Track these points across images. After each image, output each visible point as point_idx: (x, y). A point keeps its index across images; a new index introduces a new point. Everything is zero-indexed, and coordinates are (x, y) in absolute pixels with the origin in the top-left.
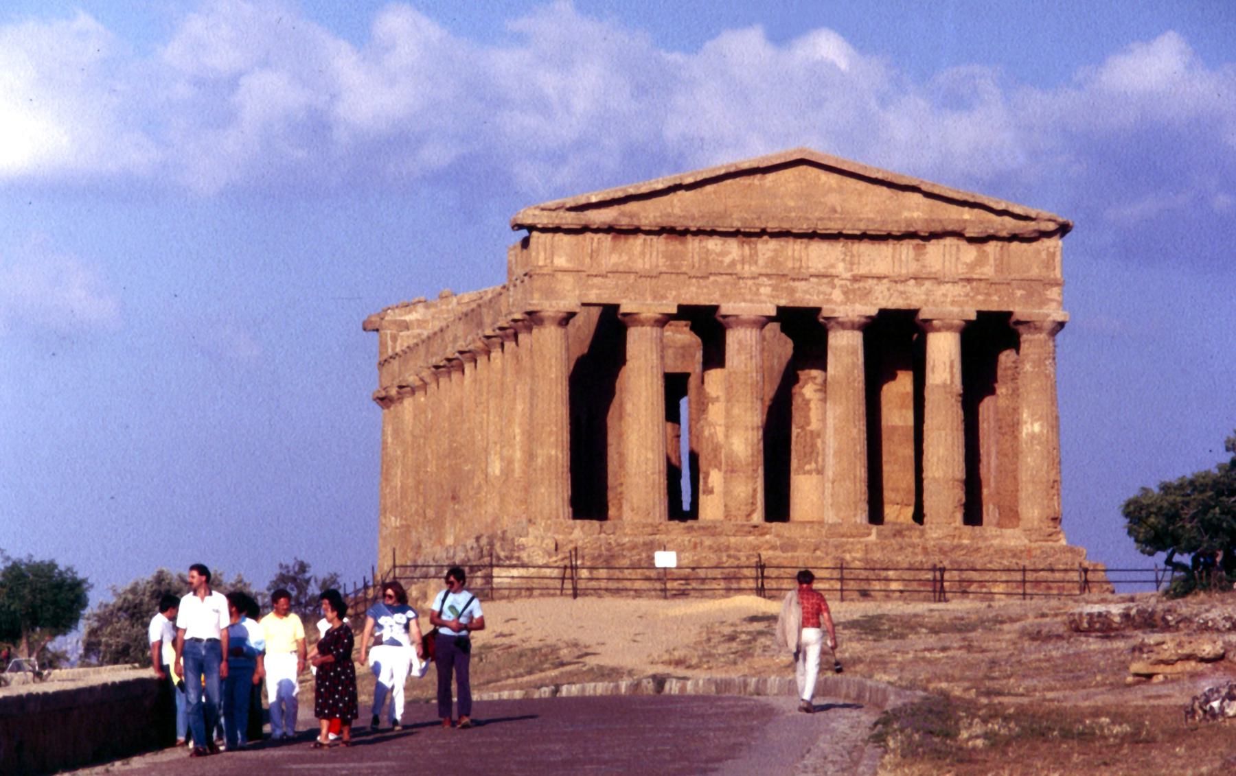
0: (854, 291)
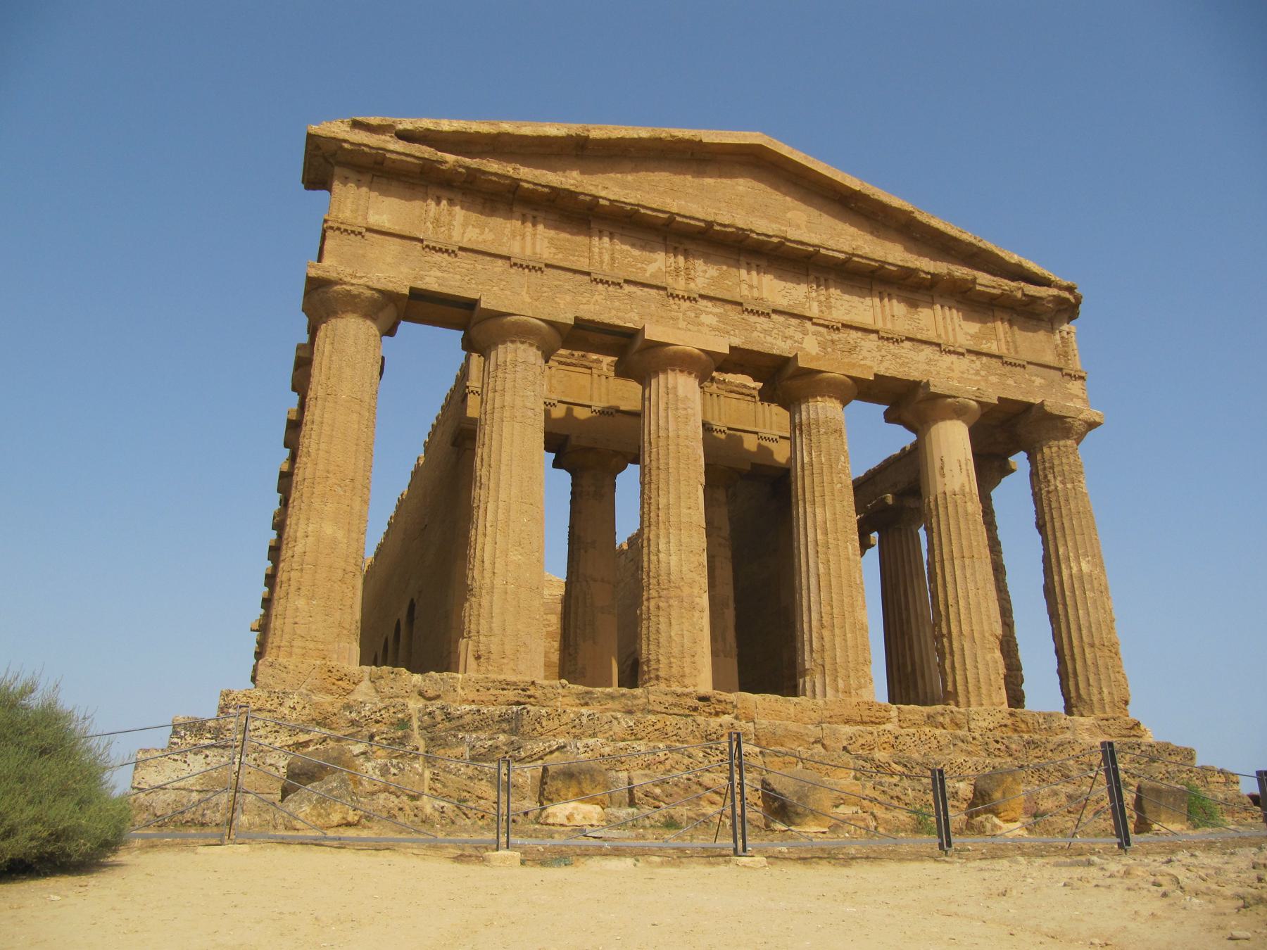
0: (833, 342)
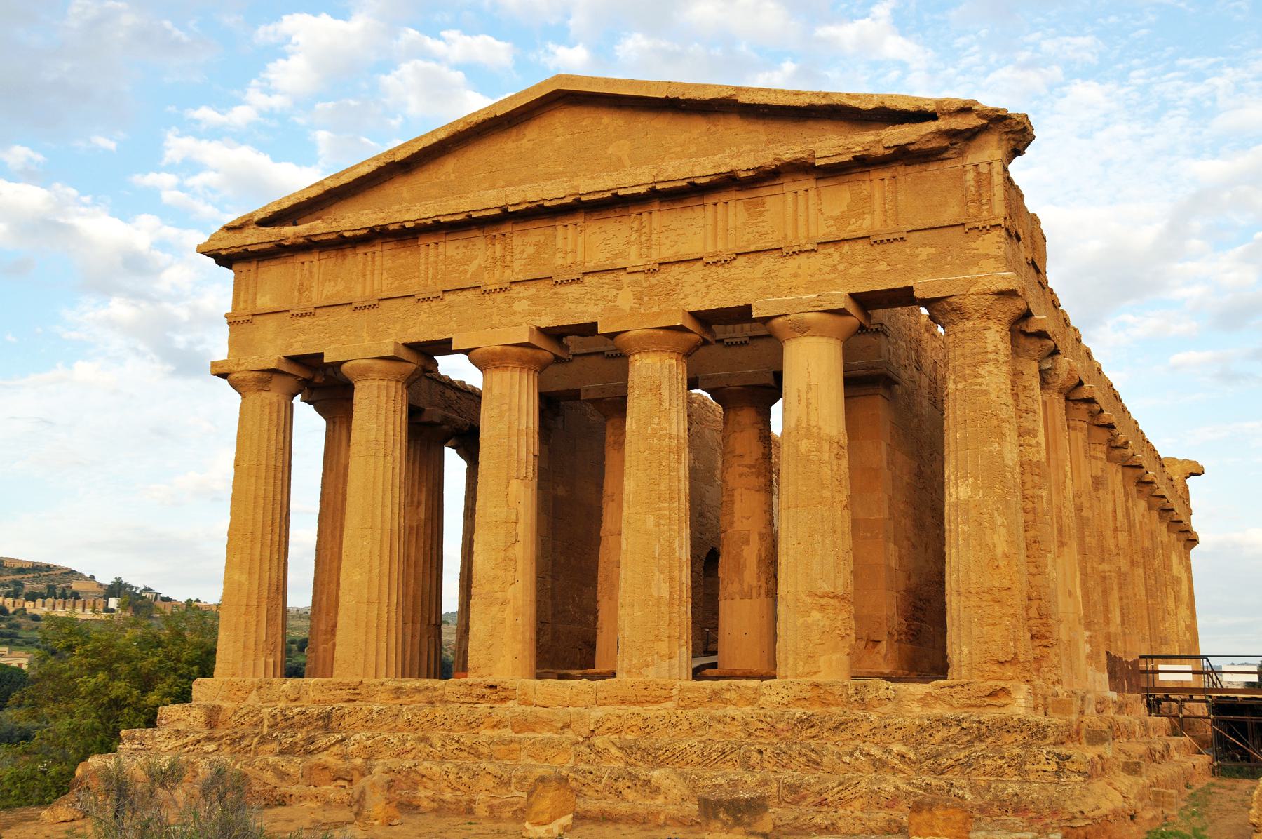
0: (650, 287)
